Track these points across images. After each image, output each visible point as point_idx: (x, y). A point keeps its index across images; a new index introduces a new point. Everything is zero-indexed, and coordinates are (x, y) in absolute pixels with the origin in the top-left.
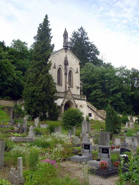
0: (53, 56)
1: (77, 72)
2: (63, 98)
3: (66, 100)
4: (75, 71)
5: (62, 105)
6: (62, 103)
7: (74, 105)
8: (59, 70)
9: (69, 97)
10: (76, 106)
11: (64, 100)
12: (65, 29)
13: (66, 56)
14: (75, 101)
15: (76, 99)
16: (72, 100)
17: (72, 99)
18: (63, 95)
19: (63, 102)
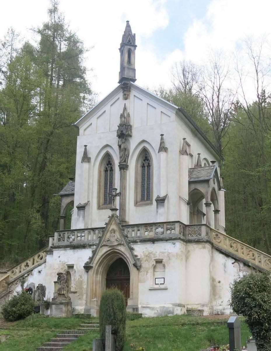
0: (85, 126)
1: (163, 148)
2: (90, 246)
3: (104, 250)
4: (157, 146)
5: (87, 268)
6: (87, 263)
7: (130, 262)
8: (108, 160)
9: (113, 239)
10: (135, 265)
11: (94, 253)
12: (125, 25)
13: (125, 109)
14: (132, 249)
15: (135, 242)
16: (122, 249)
17: (120, 244)
18: (92, 238)
19: (91, 259)
